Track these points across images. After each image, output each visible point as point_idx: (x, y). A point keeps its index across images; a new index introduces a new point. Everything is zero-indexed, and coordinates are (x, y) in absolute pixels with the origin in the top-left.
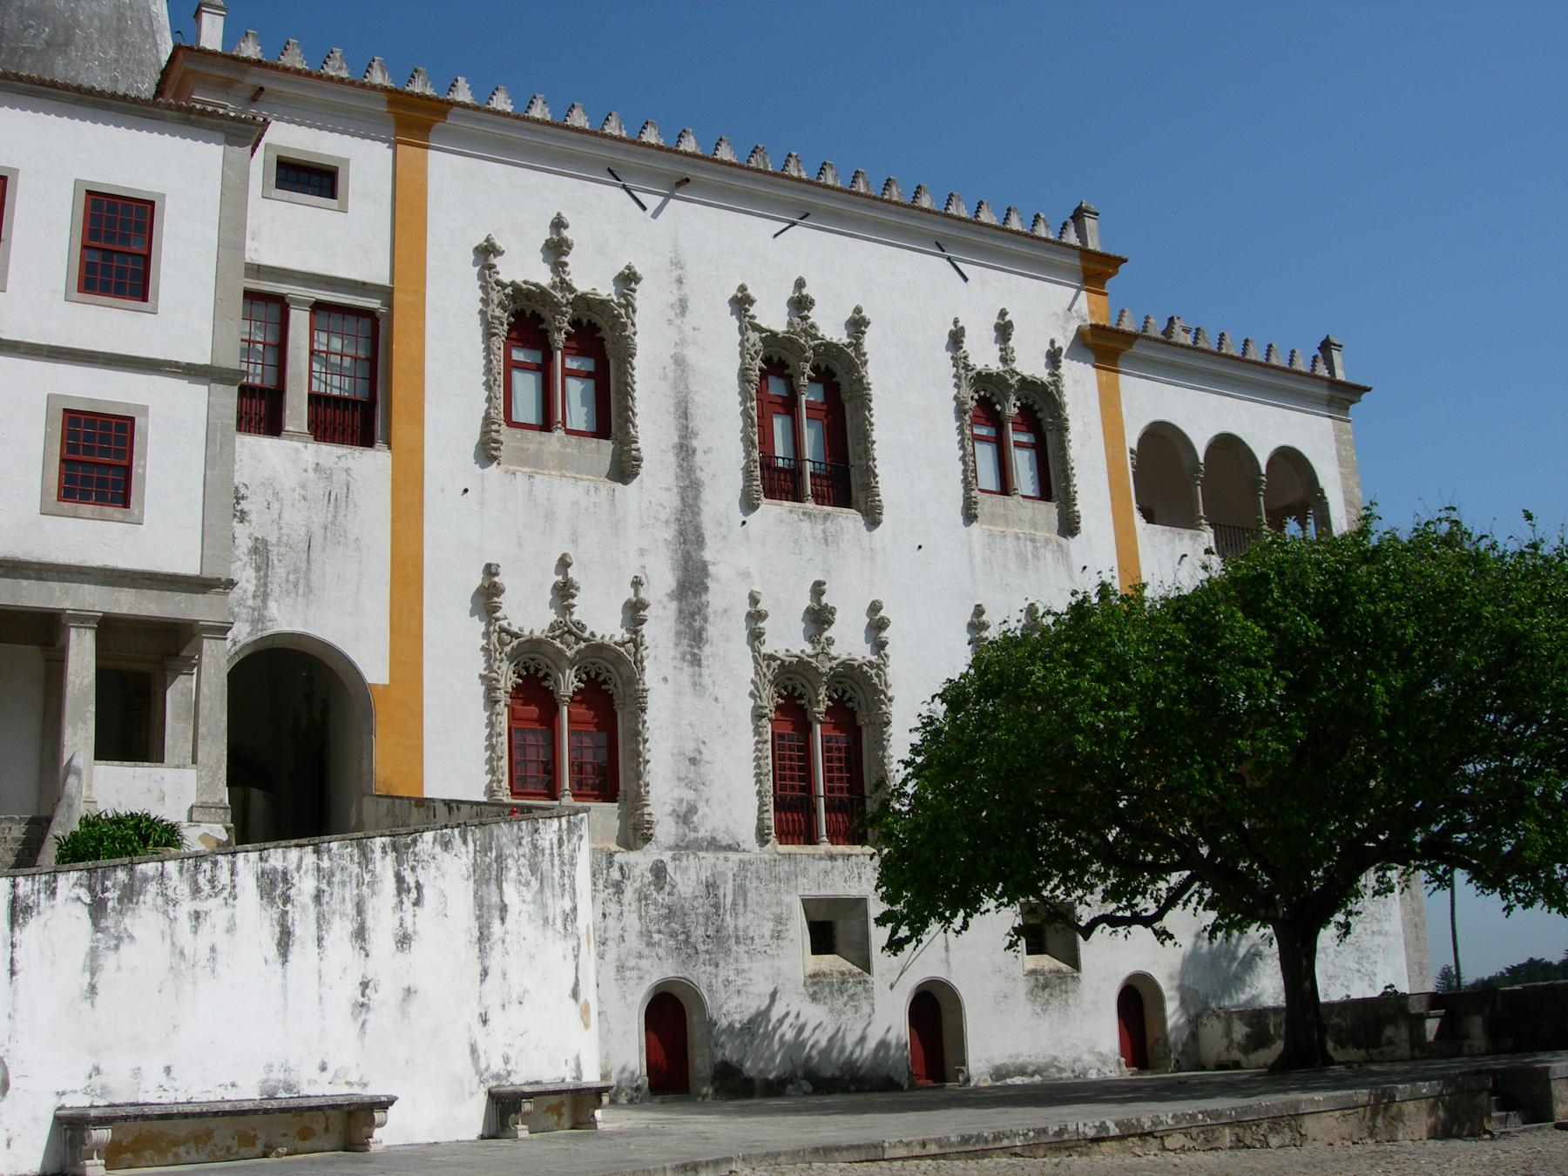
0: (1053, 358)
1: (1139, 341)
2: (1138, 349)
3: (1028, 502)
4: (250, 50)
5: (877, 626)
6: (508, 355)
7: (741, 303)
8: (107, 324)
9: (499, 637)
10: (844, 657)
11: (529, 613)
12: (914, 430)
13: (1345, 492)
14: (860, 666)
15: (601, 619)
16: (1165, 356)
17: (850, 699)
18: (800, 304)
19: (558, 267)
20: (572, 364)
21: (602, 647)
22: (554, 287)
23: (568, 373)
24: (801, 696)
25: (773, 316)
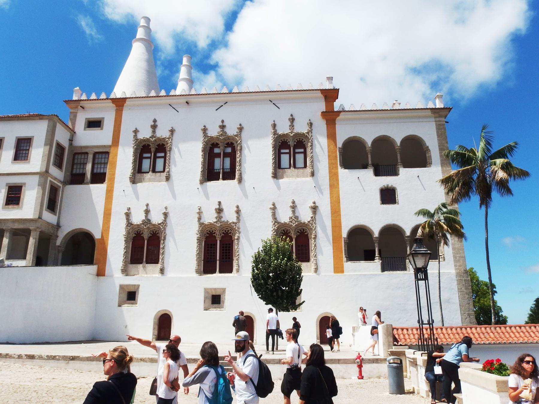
0: (311, 124)
1: (342, 113)
2: (342, 116)
3: (296, 170)
4: (84, 97)
5: (238, 212)
6: (155, 154)
7: (205, 130)
8: (21, 167)
9: (129, 224)
10: (226, 221)
11: (138, 218)
12: (256, 155)
13: (439, 146)
14: (230, 224)
15: (156, 218)
16: (388, 115)
17: (230, 233)
18: (223, 127)
19: (154, 132)
20: (159, 155)
21: (154, 225)
22: (150, 137)
23: (155, 158)
24: (215, 233)
25: (214, 132)
